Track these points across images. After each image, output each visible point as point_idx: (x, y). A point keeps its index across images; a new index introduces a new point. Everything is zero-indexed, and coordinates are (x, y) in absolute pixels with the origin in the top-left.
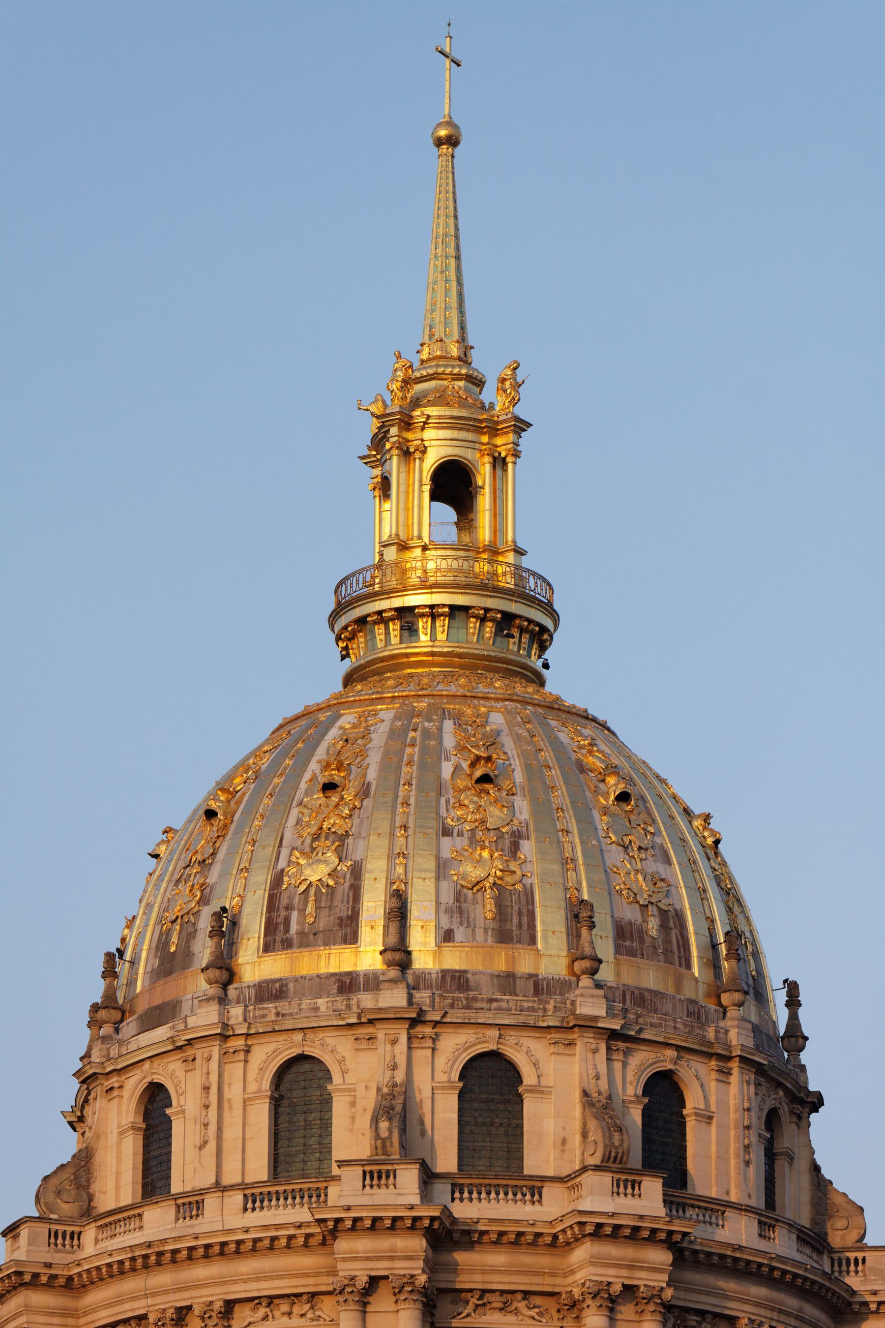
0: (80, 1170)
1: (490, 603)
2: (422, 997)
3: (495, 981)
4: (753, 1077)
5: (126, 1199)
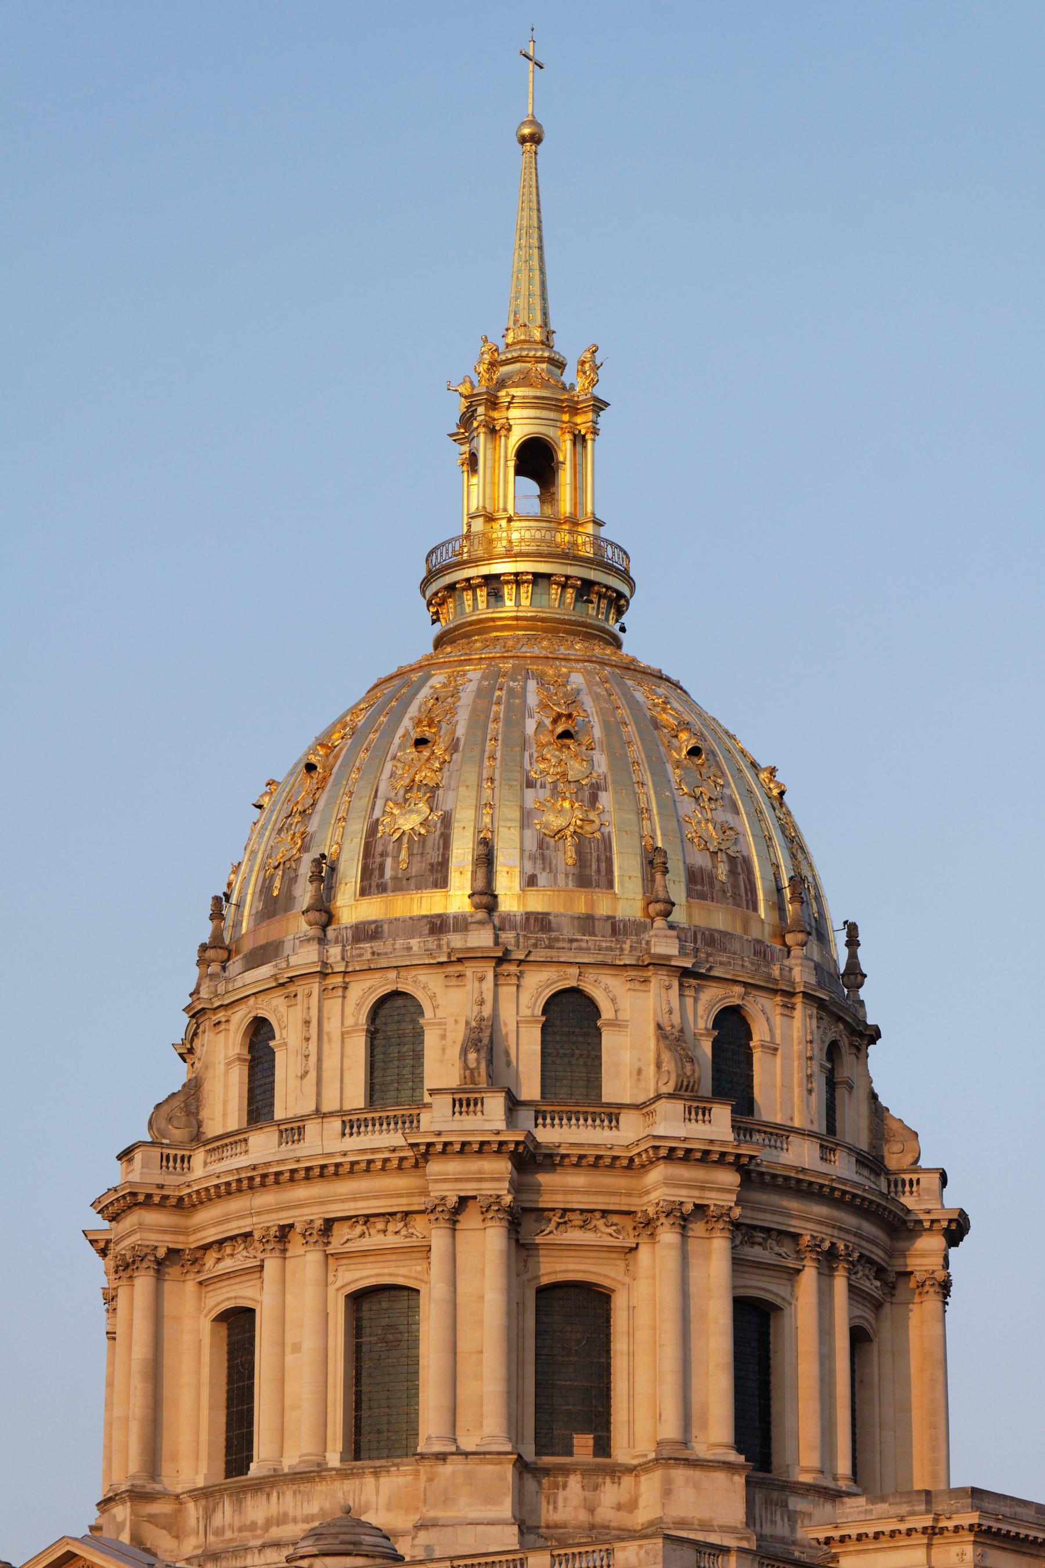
0: (190, 1098)
1: (570, 571)
2: (508, 937)
3: (576, 923)
4: (815, 1011)
5: (233, 1125)
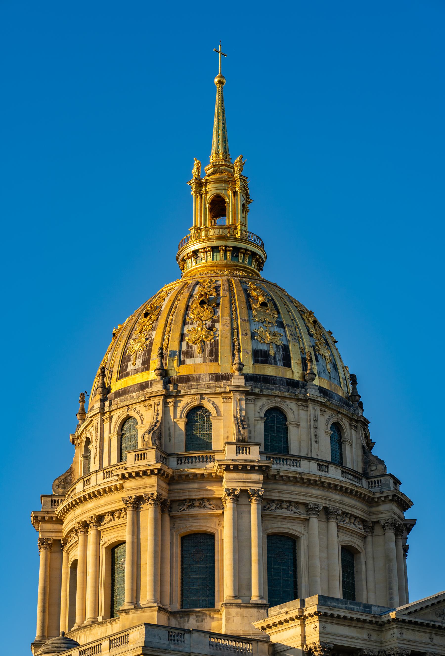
1: (226, 243)
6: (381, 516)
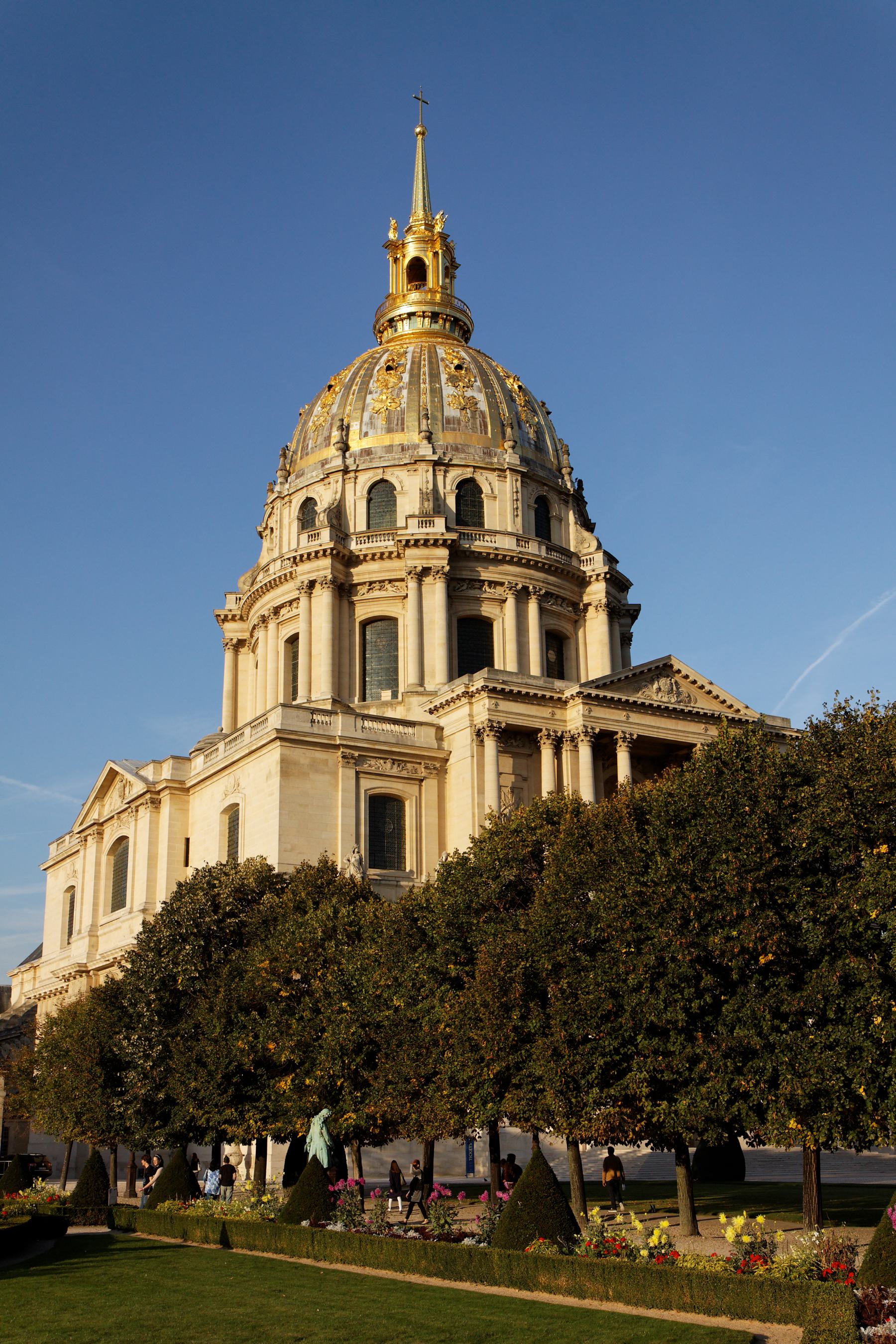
1: (424, 308)
4: (519, 478)
6: (593, 597)
